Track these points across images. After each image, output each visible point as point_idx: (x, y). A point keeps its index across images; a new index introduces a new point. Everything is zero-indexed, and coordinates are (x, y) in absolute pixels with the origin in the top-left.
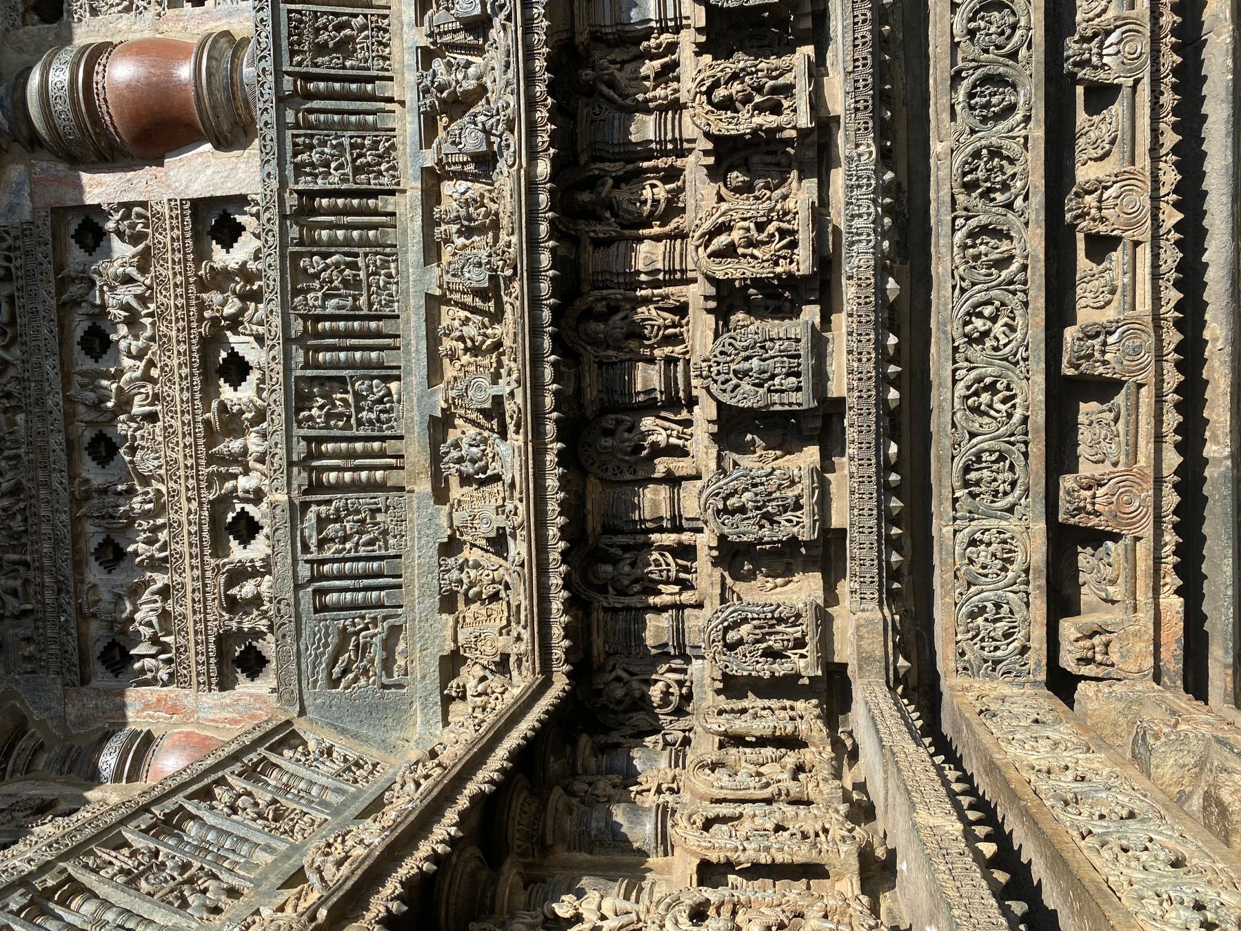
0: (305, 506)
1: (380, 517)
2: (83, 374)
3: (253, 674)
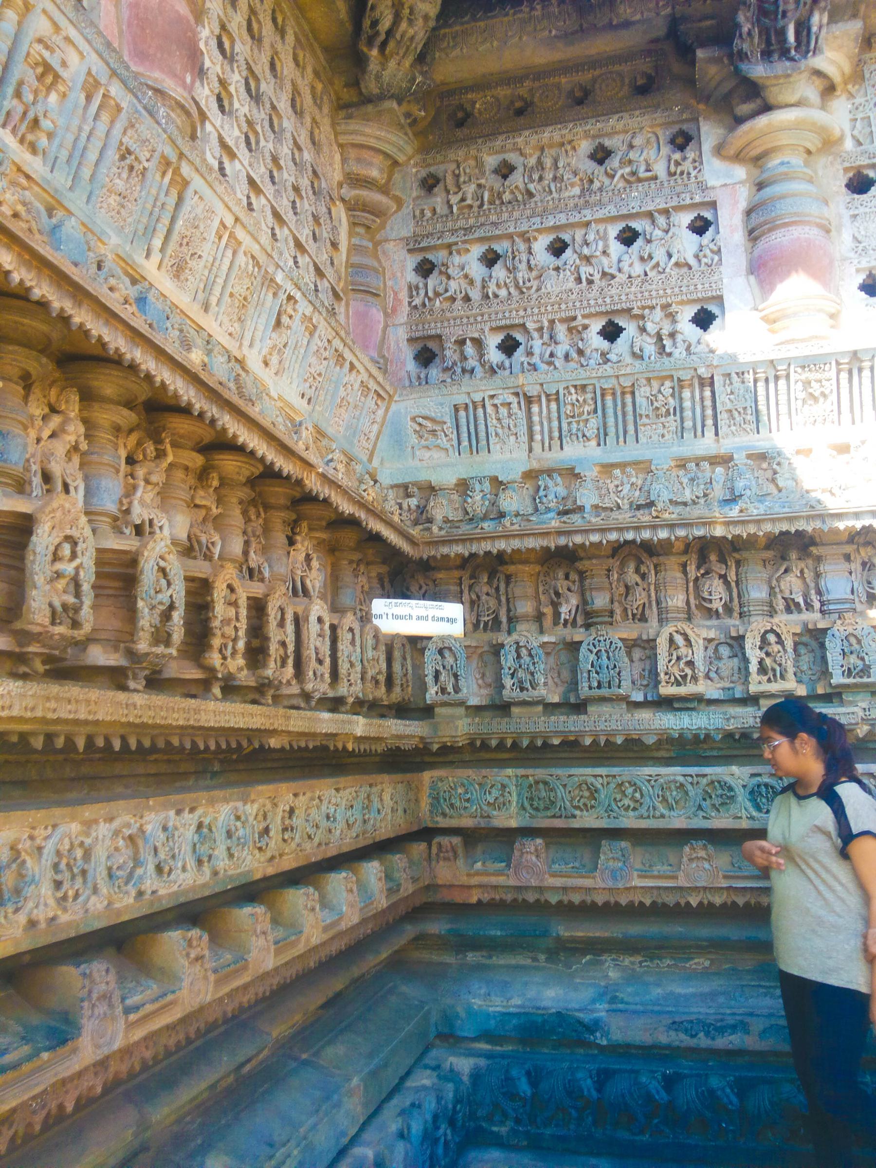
0: (517, 394)
1: (512, 438)
2: (605, 230)
3: (417, 358)
